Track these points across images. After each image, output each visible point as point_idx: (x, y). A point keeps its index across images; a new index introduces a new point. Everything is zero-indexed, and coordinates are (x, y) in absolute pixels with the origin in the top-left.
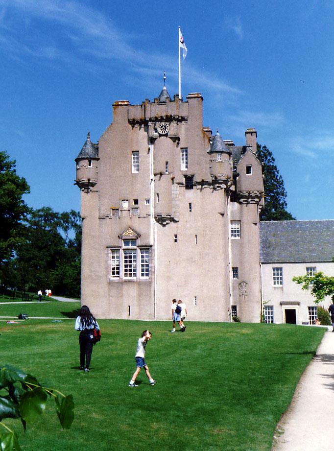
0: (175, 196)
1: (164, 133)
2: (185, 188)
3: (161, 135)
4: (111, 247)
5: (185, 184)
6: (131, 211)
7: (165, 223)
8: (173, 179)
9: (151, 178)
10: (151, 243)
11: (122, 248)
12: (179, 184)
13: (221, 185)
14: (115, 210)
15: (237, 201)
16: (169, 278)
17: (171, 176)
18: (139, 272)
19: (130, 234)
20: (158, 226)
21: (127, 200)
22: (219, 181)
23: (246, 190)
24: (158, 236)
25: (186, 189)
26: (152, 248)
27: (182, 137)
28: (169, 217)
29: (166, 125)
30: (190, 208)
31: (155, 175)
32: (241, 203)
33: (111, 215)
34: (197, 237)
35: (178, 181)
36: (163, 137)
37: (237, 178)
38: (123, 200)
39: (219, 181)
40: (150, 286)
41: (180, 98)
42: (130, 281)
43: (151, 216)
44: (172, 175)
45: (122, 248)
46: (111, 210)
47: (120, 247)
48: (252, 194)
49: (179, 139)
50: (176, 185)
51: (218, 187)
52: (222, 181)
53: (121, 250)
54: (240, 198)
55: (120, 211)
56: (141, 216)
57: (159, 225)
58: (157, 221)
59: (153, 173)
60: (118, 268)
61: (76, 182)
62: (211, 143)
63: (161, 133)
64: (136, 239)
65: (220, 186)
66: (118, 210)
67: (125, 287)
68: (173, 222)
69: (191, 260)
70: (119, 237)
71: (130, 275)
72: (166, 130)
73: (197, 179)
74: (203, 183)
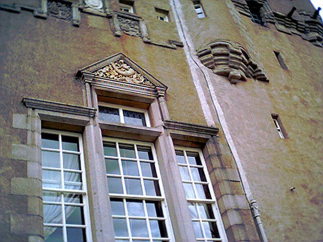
10: (210, 122)
24: (225, 106)
43: (185, 47)
57: (219, 79)
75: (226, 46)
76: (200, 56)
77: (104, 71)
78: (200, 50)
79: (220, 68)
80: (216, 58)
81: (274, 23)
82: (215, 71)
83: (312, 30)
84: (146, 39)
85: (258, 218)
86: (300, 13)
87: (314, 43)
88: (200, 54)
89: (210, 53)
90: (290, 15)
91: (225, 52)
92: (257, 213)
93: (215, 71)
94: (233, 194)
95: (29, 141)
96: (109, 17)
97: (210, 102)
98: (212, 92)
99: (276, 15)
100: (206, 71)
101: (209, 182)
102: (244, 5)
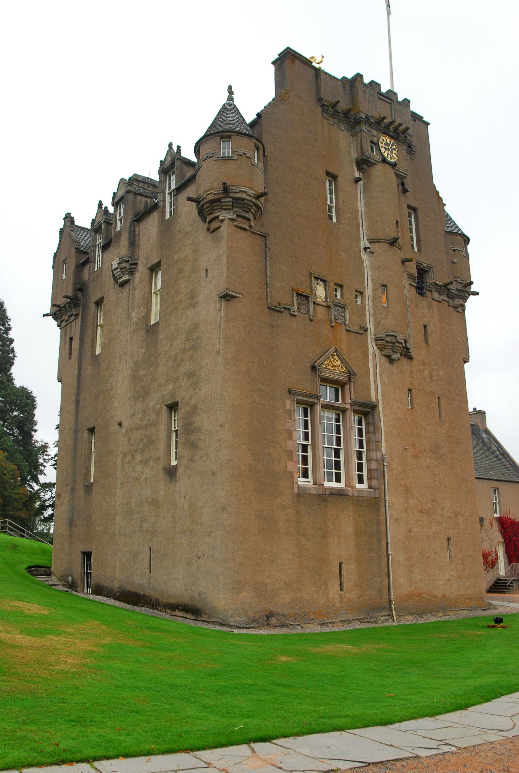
3: (384, 160)
9: (362, 246)
20: (380, 361)
24: (383, 384)
31: (371, 241)
38: (317, 278)
40: (379, 511)
43: (369, 332)
58: (381, 349)
59: (365, 238)
73: (432, 278)
75: (395, 337)
78: (378, 336)
79: (387, 352)
80: (387, 344)
81: (431, 291)
82: (383, 353)
84: (348, 328)
85: (386, 467)
86: (455, 279)
87: (456, 309)
88: (376, 339)
89: (383, 340)
90: (445, 285)
91: (393, 341)
92: (385, 464)
93: (383, 353)
94: (376, 451)
95: (293, 418)
96: (328, 307)
97: (375, 382)
98: (378, 372)
99: (436, 284)
100: (377, 353)
101: (364, 438)
102: (414, 277)
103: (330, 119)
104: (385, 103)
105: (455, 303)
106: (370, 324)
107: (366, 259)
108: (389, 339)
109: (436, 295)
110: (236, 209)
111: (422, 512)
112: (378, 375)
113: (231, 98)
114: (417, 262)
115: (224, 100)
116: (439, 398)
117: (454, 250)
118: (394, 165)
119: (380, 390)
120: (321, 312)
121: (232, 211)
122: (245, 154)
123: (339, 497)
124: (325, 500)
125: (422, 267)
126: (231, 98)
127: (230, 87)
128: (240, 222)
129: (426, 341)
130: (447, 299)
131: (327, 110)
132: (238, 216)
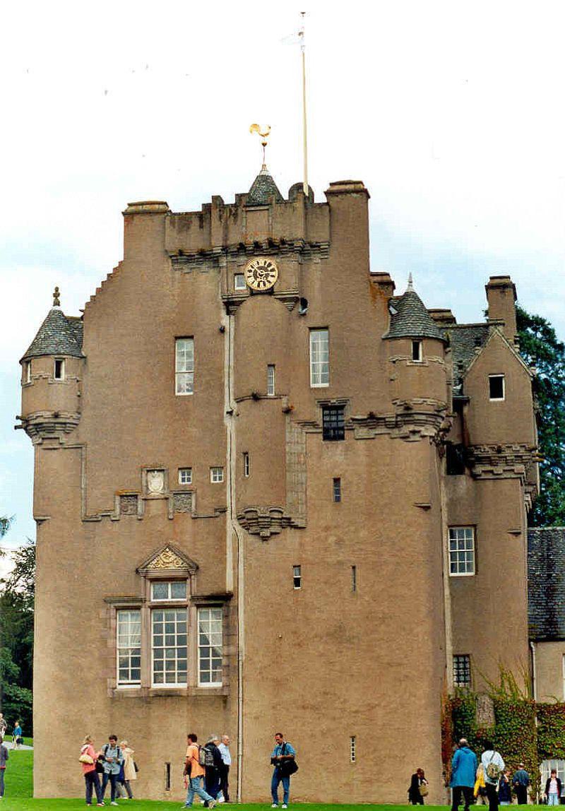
0: (295, 459)
1: (262, 288)
2: (321, 436)
3: (253, 293)
4: (115, 602)
5: (321, 426)
6: (171, 501)
7: (266, 533)
8: (288, 411)
9: (227, 409)
10: (229, 587)
11: (148, 604)
12: (305, 424)
13: (422, 429)
14: (130, 497)
15: (467, 471)
16: (279, 684)
17: (284, 403)
18: (195, 669)
19: (169, 563)
21: (163, 470)
22: (417, 417)
23: (490, 441)
24: (248, 566)
25: (324, 439)
26: (232, 603)
27: (315, 296)
28: (276, 515)
29: (270, 265)
30: (337, 492)
31: (239, 400)
32: (475, 477)
33: (118, 510)
34: (357, 570)
35: (302, 417)
36: (259, 297)
37: (466, 410)
38: (148, 471)
39: (417, 417)
41: (307, 194)
42: (169, 695)
44: (284, 400)
45: (148, 604)
46: (118, 498)
47: (143, 601)
48: (507, 453)
49: (304, 303)
50: (297, 429)
51: (414, 432)
52: (423, 417)
53: (143, 609)
54: (471, 466)
55: (140, 503)
56: (202, 513)
57: (252, 539)
58: (246, 527)
59: (232, 398)
60: (136, 662)
61: (19, 423)
62: (394, 312)
63: (255, 286)
64: (185, 579)
65: (419, 432)
66: (136, 496)
67: (157, 711)
68: (289, 529)
69: (338, 634)
70: (137, 571)
71: (170, 678)
72: (270, 279)
74: (373, 420)
76: (239, 519)
77: (154, 562)
79: (253, 529)
83: (407, 423)
84: (193, 516)
86: (394, 402)
89: (244, 518)
93: (250, 532)
96: (166, 499)
97: (236, 568)
103: (185, 267)
104: (259, 212)
105: (402, 432)
106: (230, 501)
107: (230, 424)
108: (249, 516)
109: (362, 432)
110: (41, 433)
111: (304, 707)
112: (241, 558)
113: (57, 303)
114: (319, 402)
115: (48, 306)
116: (354, 568)
117: (394, 362)
118: (270, 292)
119: (241, 576)
120: (156, 507)
121: (38, 436)
122: (41, 376)
123: (169, 700)
124: (150, 703)
125: (330, 404)
126: (57, 303)
127: (57, 289)
128: (47, 444)
129: (338, 499)
130: (384, 430)
131: (177, 260)
132: (43, 439)
